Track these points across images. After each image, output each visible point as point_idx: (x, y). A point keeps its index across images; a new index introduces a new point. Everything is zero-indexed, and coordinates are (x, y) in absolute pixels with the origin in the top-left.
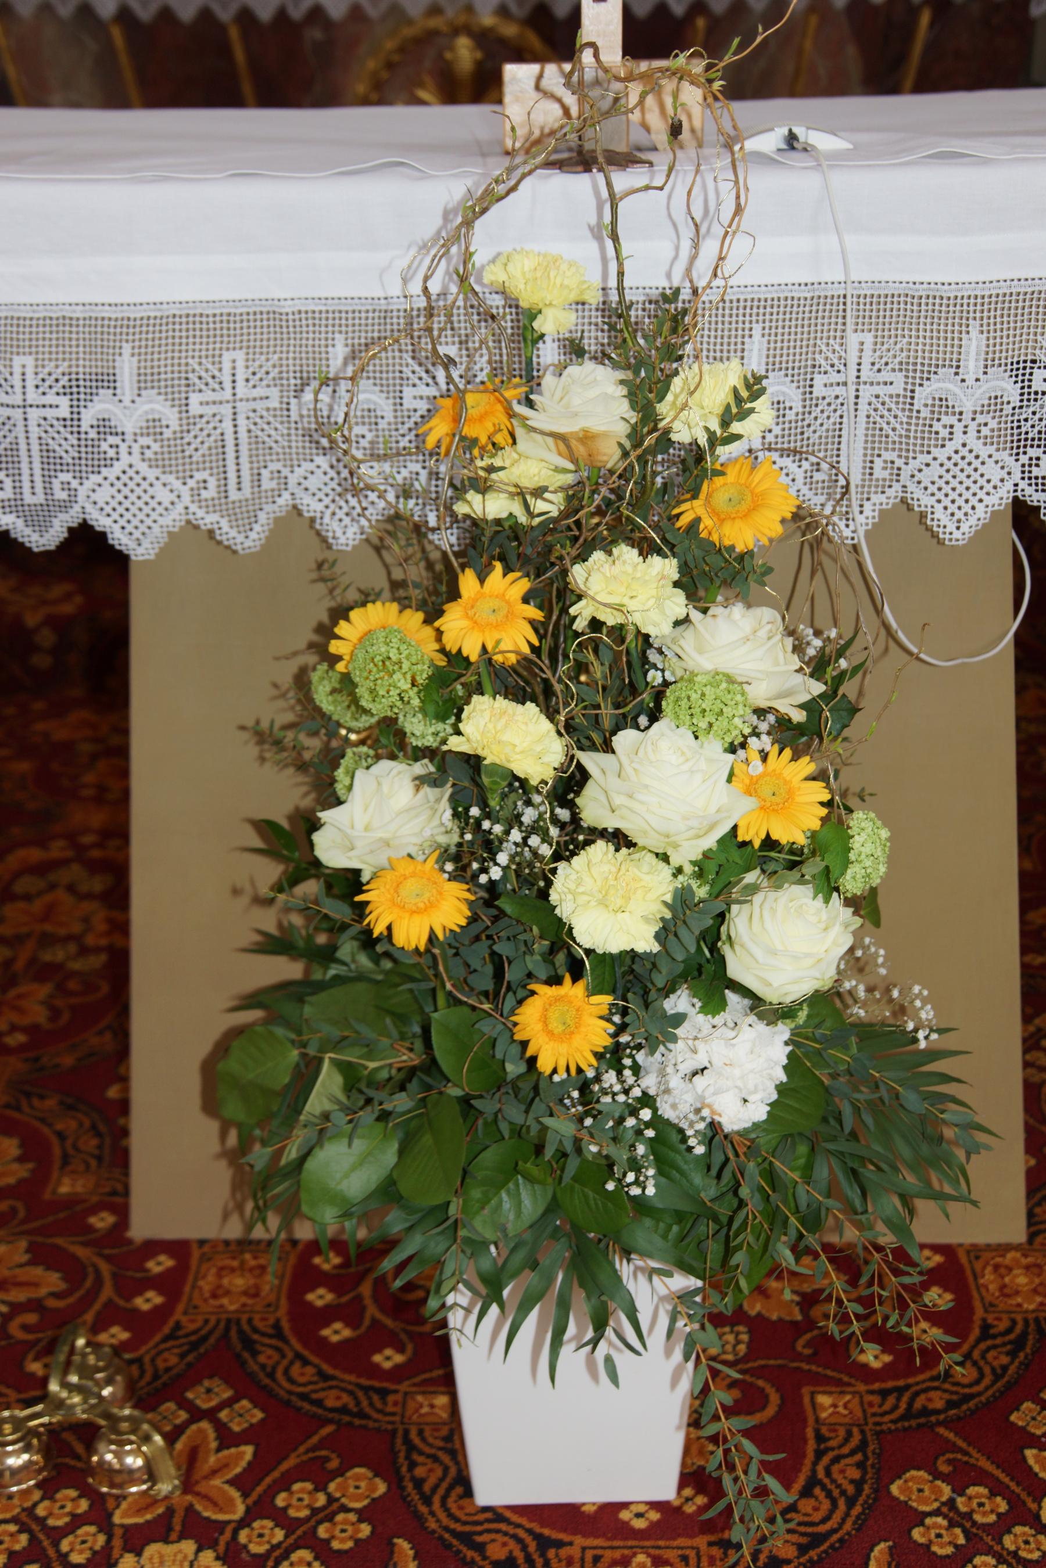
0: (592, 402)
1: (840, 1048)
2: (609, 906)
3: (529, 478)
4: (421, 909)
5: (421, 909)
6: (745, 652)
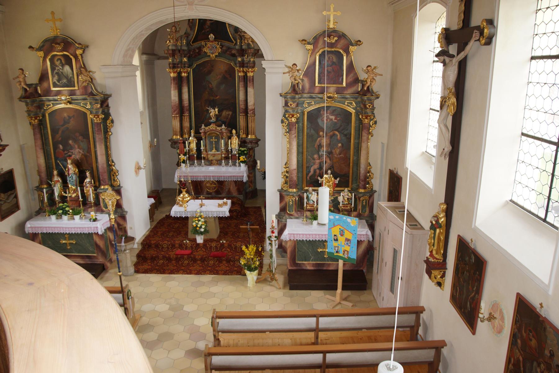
0: (199, 214)
2: (199, 226)
3: (198, 216)
4: (195, 226)
6: (203, 220)
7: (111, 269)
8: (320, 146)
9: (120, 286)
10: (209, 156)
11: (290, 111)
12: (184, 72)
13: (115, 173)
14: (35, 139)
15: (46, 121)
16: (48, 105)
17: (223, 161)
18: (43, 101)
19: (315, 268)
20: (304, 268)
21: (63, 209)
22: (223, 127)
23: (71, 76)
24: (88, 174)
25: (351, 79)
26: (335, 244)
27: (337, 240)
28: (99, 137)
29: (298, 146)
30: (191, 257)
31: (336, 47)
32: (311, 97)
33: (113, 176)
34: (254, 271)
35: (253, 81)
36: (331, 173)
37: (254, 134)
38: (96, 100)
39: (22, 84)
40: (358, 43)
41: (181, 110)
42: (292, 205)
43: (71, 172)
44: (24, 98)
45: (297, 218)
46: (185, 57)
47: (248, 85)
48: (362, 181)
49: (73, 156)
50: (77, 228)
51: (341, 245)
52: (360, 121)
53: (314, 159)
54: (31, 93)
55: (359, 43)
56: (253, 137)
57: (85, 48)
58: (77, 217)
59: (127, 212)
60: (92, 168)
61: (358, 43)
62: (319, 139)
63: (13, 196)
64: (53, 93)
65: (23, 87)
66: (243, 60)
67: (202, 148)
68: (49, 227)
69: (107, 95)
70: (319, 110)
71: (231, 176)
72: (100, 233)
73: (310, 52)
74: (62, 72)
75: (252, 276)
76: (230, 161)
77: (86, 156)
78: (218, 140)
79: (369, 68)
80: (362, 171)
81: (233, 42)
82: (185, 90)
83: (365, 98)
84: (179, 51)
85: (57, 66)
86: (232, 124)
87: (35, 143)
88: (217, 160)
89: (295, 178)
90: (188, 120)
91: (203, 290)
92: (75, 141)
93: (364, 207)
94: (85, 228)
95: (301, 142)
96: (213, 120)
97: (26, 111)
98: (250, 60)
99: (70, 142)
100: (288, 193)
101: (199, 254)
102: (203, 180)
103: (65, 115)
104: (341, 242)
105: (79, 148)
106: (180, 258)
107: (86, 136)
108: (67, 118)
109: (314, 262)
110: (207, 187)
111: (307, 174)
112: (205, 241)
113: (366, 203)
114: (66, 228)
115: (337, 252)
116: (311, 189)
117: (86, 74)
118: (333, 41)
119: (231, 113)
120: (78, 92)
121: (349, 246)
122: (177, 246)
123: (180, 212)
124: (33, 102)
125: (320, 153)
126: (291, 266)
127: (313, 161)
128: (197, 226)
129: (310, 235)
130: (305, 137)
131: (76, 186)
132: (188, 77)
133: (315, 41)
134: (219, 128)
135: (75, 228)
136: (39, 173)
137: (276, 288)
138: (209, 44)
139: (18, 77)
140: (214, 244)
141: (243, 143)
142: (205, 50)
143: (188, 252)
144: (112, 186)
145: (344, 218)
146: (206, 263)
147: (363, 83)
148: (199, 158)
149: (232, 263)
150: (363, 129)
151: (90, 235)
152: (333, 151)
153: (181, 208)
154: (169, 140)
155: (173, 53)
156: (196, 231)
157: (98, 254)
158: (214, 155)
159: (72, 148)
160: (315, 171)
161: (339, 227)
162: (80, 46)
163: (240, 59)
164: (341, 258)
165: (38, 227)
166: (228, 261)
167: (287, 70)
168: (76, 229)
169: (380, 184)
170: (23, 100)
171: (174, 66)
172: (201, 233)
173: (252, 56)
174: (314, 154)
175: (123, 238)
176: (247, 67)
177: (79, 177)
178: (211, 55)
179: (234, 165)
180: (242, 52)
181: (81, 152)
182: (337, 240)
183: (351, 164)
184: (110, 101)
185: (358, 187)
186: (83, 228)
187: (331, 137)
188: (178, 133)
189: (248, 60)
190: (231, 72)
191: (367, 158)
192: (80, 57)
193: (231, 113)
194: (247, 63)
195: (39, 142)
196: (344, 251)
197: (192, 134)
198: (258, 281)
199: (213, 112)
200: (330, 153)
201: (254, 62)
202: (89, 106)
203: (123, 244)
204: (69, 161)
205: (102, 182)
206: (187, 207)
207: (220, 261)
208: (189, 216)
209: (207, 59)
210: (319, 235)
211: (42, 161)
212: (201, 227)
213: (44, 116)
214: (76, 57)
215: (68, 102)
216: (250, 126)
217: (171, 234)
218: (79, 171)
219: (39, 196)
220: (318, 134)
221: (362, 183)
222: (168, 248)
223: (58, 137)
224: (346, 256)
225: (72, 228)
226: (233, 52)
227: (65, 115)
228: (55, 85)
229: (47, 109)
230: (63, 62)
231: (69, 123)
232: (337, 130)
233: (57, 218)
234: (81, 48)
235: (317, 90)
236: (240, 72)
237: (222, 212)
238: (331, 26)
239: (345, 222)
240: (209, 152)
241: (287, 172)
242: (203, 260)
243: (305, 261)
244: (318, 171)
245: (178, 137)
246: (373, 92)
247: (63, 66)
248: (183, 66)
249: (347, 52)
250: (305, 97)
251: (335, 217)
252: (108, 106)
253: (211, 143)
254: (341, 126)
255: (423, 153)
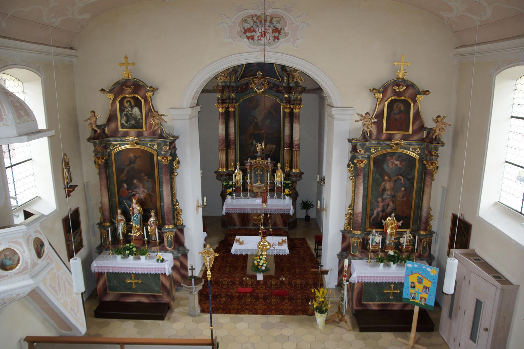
1: (266, 267)
2: (261, 264)
3: (259, 254)
4: (256, 264)
5: (256, 264)
7: (177, 307)
8: (384, 190)
9: (210, 338)
10: (254, 188)
11: (359, 157)
12: (232, 108)
13: (178, 212)
14: (100, 178)
15: (112, 160)
16: (114, 146)
17: (269, 194)
18: (110, 141)
19: (380, 308)
20: (369, 308)
21: (130, 249)
22: (269, 160)
23: (139, 117)
24: (153, 214)
25: (416, 127)
26: (412, 291)
27: (414, 287)
28: (165, 178)
29: (364, 189)
30: (254, 295)
31: (403, 96)
32: (379, 144)
33: (177, 215)
34: (325, 313)
35: (299, 118)
36: (395, 216)
37: (298, 168)
38: (166, 142)
39: (94, 126)
40: (426, 93)
41: (227, 143)
42: (357, 246)
43: (136, 211)
44: (92, 139)
45: (361, 259)
46: (233, 93)
47: (294, 121)
48: (424, 224)
49: (137, 195)
50: (144, 268)
51: (419, 293)
52: (424, 167)
53: (378, 202)
54: (99, 134)
55: (427, 93)
56: (297, 170)
57: (154, 90)
58: (143, 257)
59: (188, 250)
60: (156, 207)
61: (426, 93)
62: (383, 183)
63: (78, 234)
64: (120, 134)
65: (93, 129)
66: (289, 97)
67: (248, 181)
68: (115, 267)
69: (173, 136)
70: (384, 155)
71: (278, 209)
72: (167, 274)
73: (379, 100)
74: (131, 114)
75: (320, 318)
76: (275, 194)
77: (150, 195)
78: (264, 173)
79: (439, 119)
80: (424, 214)
81: (279, 80)
82: (232, 124)
83: (433, 146)
84: (228, 87)
85: (126, 108)
86: (276, 158)
87: (100, 182)
88: (262, 193)
89: (360, 221)
90: (234, 153)
91: (275, 332)
92: (140, 180)
93: (424, 248)
94: (152, 268)
95: (366, 186)
96: (259, 154)
97: (93, 151)
98: (297, 98)
99: (135, 181)
100: (352, 235)
101: (261, 292)
102: (251, 212)
103: (132, 155)
104: (419, 290)
105: (143, 187)
106: (243, 296)
107: (151, 175)
108: (134, 158)
109: (380, 303)
110: (254, 219)
111: (371, 217)
112: (265, 277)
113: (426, 244)
114: (132, 268)
115: (413, 298)
116: (374, 231)
117: (158, 118)
118: (401, 90)
119: (274, 146)
120: (145, 134)
121: (427, 293)
122: (237, 283)
123: (240, 250)
124: (101, 143)
125: (384, 197)
126: (357, 306)
127: (376, 204)
128: (258, 265)
129: (377, 277)
130: (371, 181)
131: (140, 225)
132: (234, 112)
133: (384, 90)
134: (265, 162)
135: (141, 268)
136: (102, 209)
137: (346, 329)
138: (257, 81)
139: (89, 119)
140: (274, 282)
141: (288, 176)
142: (252, 86)
143: (249, 289)
144: (175, 225)
145: (424, 267)
146: (269, 301)
147: (430, 131)
148: (245, 190)
149: (294, 302)
150: (426, 174)
151: (157, 276)
152: (397, 194)
153: (241, 246)
154: (215, 172)
155: (223, 89)
156: (257, 269)
157: (163, 293)
158: (259, 188)
159: (136, 187)
160: (378, 214)
161: (417, 275)
162: (151, 89)
163: (286, 96)
164: (417, 304)
165: (104, 267)
166: (290, 299)
167: (359, 118)
168: (143, 269)
169: (441, 228)
170: (92, 141)
171: (222, 102)
172: (263, 271)
173: (299, 93)
174: (378, 198)
175: (193, 279)
176: (294, 104)
177: (143, 215)
178: (258, 91)
179: (279, 197)
180: (289, 90)
181: (146, 191)
182: (414, 287)
183: (413, 207)
184: (177, 142)
185: (419, 229)
186: (150, 268)
187: (395, 181)
188: (224, 166)
189: (295, 97)
190: (276, 108)
191: (429, 203)
192: (150, 99)
193: (274, 146)
194: (294, 100)
195: (104, 182)
196: (421, 298)
197: (238, 167)
198: (327, 322)
199: (260, 147)
200: (393, 197)
201: (301, 99)
202: (156, 147)
203: (193, 286)
204: (134, 201)
205: (167, 222)
206: (246, 244)
207: (283, 300)
208: (249, 253)
209: (253, 95)
210: (386, 277)
211: (106, 200)
212: (262, 265)
213: (110, 155)
214: (146, 99)
215: (136, 143)
216: (294, 159)
217: (228, 269)
218: (144, 210)
219: (101, 234)
220: (383, 178)
221: (423, 225)
222: (228, 284)
223: (123, 176)
224: (423, 303)
225: (138, 268)
226: (280, 89)
227: (132, 155)
228: (123, 126)
229: (113, 149)
230: (132, 103)
231: (134, 163)
232: (401, 175)
233: (122, 258)
234: (152, 91)
235: (384, 137)
236: (287, 108)
237: (282, 250)
238: (401, 76)
239: (425, 271)
240: (254, 185)
241: (351, 214)
242: (265, 298)
243: (371, 301)
244: (381, 214)
245: (224, 170)
246: (440, 140)
247: (132, 107)
248: (231, 101)
249: (415, 101)
250: (373, 144)
251: (413, 266)
252: (174, 147)
253: (256, 176)
254: (405, 171)
255: (496, 203)
